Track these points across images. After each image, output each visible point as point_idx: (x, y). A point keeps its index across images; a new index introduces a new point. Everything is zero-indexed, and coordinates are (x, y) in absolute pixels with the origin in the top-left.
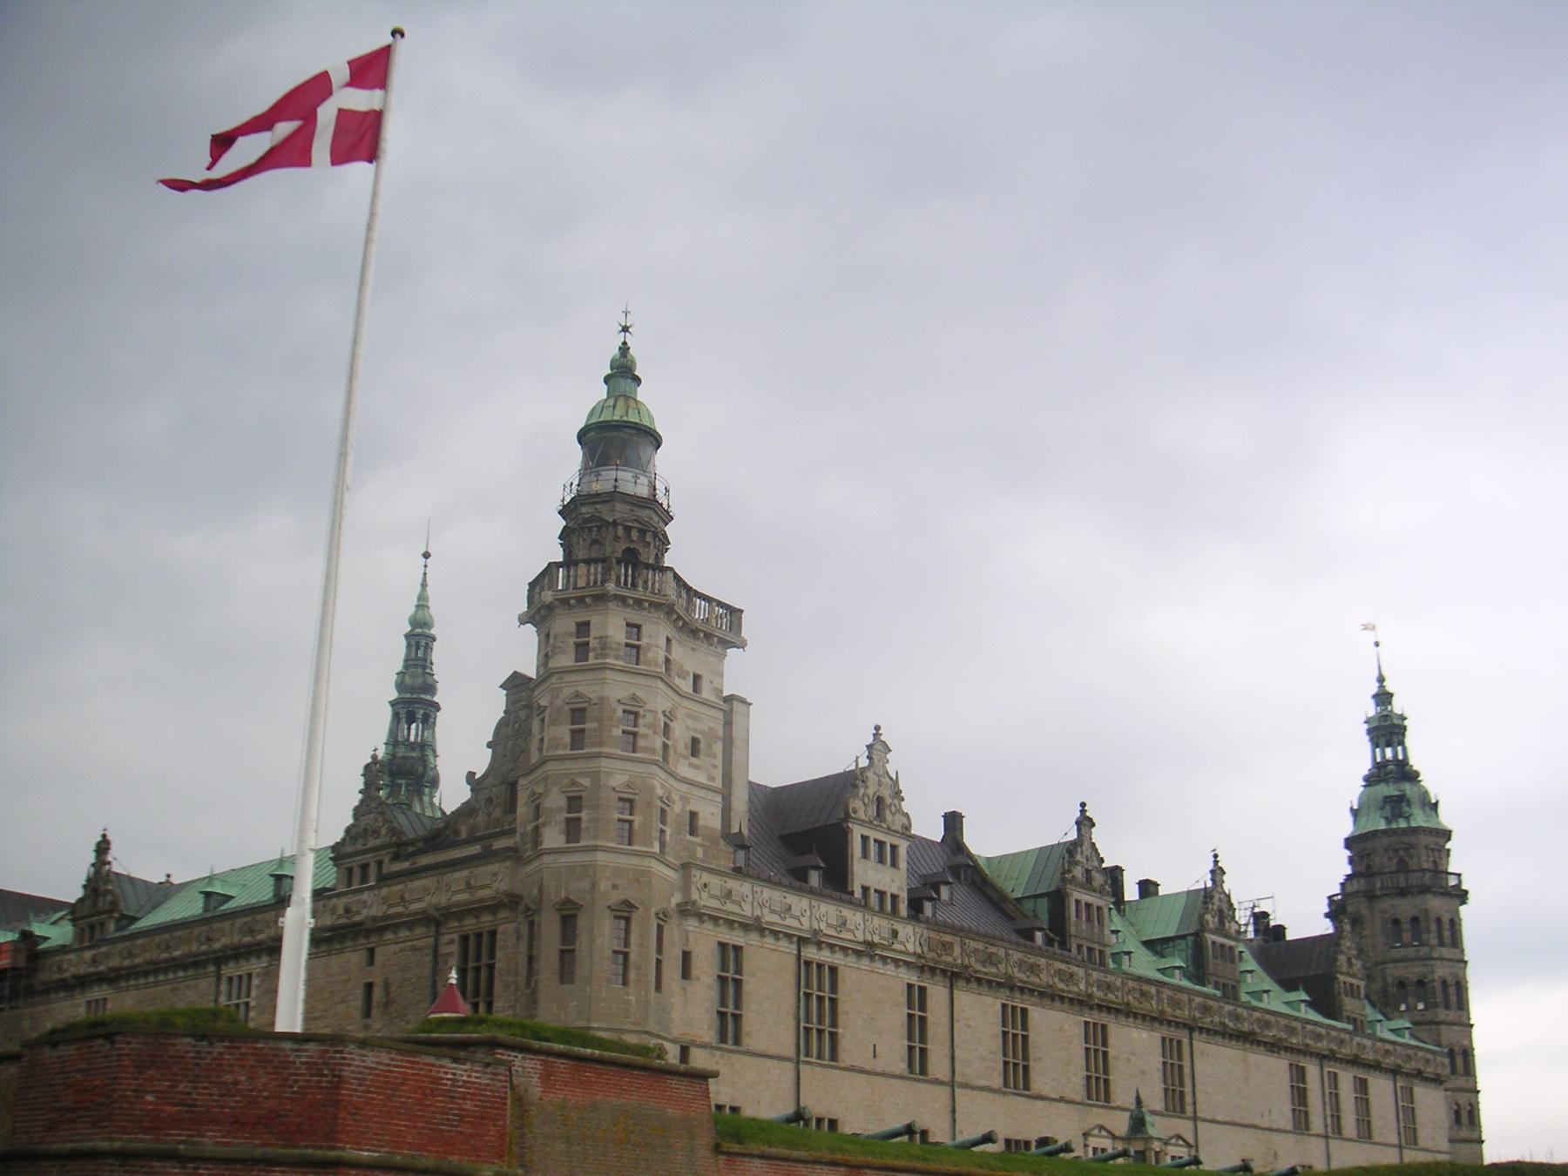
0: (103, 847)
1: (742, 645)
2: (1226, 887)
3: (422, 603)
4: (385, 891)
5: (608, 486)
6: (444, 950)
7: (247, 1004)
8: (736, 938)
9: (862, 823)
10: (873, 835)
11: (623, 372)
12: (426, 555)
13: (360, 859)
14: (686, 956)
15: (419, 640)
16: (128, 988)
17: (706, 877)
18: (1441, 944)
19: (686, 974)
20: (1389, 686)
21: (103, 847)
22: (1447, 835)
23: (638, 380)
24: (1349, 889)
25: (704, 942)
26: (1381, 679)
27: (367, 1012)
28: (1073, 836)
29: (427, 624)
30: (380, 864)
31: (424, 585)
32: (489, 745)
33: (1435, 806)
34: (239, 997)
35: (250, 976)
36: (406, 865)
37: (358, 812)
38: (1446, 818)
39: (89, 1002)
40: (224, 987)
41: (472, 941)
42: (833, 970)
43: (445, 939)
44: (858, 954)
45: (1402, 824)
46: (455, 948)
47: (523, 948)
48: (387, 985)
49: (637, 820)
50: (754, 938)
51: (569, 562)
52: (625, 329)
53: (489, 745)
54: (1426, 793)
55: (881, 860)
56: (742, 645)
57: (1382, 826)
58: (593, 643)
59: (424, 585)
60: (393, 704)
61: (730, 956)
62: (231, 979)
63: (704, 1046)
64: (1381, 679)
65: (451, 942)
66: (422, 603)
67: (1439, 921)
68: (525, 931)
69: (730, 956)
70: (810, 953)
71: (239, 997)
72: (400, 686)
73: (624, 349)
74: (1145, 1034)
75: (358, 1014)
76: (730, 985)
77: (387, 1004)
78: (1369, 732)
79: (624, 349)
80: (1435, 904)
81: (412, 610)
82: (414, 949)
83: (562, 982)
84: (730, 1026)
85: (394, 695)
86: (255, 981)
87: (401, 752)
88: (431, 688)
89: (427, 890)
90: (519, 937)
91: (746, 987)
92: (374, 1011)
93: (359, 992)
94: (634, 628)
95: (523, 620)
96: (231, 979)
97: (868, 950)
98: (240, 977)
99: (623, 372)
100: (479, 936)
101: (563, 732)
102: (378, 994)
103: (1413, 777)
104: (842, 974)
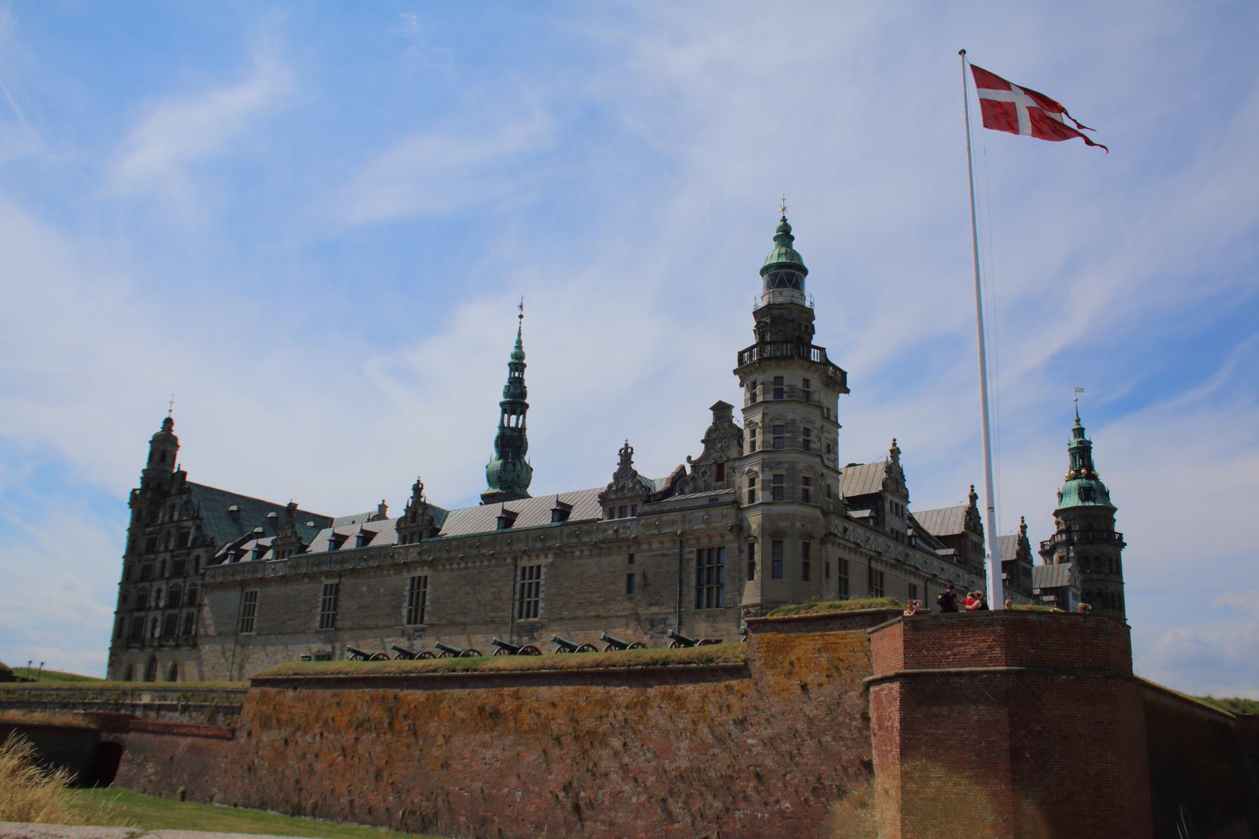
0: (418, 489)
1: (847, 391)
2: (1028, 535)
3: (519, 342)
4: (643, 522)
5: (788, 300)
6: (686, 556)
7: (538, 584)
8: (846, 555)
9: (892, 493)
11: (785, 236)
12: (521, 317)
13: (620, 503)
14: (827, 564)
15: (518, 364)
16: (444, 570)
18: (1111, 572)
19: (827, 576)
20: (1083, 424)
21: (418, 489)
22: (1114, 510)
23: (793, 238)
24: (1058, 538)
26: (1078, 421)
27: (630, 589)
28: (967, 502)
30: (634, 507)
31: (520, 334)
32: (703, 441)
33: (1105, 494)
34: (531, 578)
35: (539, 567)
36: (655, 507)
37: (616, 476)
38: (1114, 500)
39: (413, 579)
40: (519, 572)
41: (705, 554)
42: (882, 574)
43: (687, 550)
44: (892, 566)
45: (1092, 504)
46: (694, 556)
47: (745, 555)
48: (644, 576)
49: (811, 489)
51: (761, 343)
52: (784, 210)
53: (703, 441)
54: (1102, 487)
55: (897, 514)
56: (847, 391)
57: (1080, 504)
58: (786, 389)
59: (520, 334)
60: (502, 404)
61: (843, 564)
62: (524, 569)
64: (1078, 421)
65: (692, 552)
66: (519, 342)
67: (1110, 559)
68: (746, 548)
69: (843, 564)
70: (874, 565)
71: (531, 578)
72: (506, 394)
73: (784, 220)
75: (624, 591)
77: (645, 586)
78: (1070, 450)
79: (784, 220)
80: (1109, 549)
82: (664, 555)
83: (773, 577)
85: (503, 399)
86: (543, 570)
87: (508, 433)
88: (523, 395)
89: (674, 522)
90: (741, 551)
91: (850, 582)
92: (636, 590)
93: (625, 578)
94: (806, 382)
95: (736, 372)
96: (524, 569)
98: (531, 568)
99: (785, 236)
100: (710, 551)
101: (770, 437)
102: (638, 580)
103: (1095, 478)
104: (887, 578)
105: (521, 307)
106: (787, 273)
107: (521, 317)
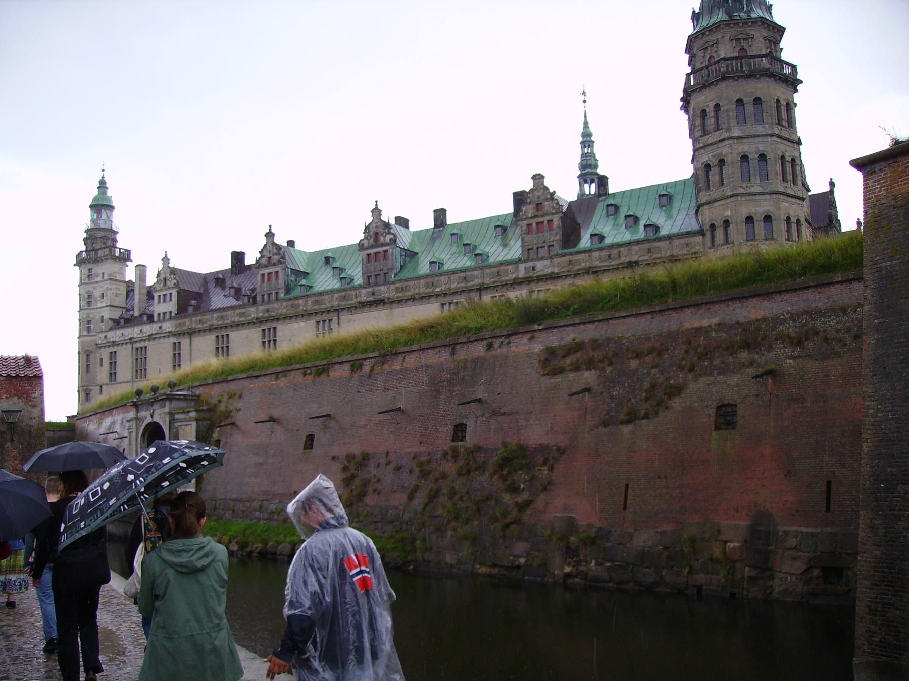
3: (586, 123)
8: (112, 349)
10: (162, 293)
11: (102, 185)
15: (587, 141)
17: (100, 335)
19: (101, 365)
25: (105, 354)
29: (590, 135)
31: (585, 116)
50: (120, 347)
59: (585, 116)
63: (107, 384)
66: (586, 123)
69: (113, 355)
73: (103, 177)
74: (303, 324)
76: (113, 364)
79: (103, 177)
81: (582, 130)
84: (113, 376)
97: (151, 337)
99: (102, 185)
105: (584, 93)
106: (101, 206)
107: (585, 102)
